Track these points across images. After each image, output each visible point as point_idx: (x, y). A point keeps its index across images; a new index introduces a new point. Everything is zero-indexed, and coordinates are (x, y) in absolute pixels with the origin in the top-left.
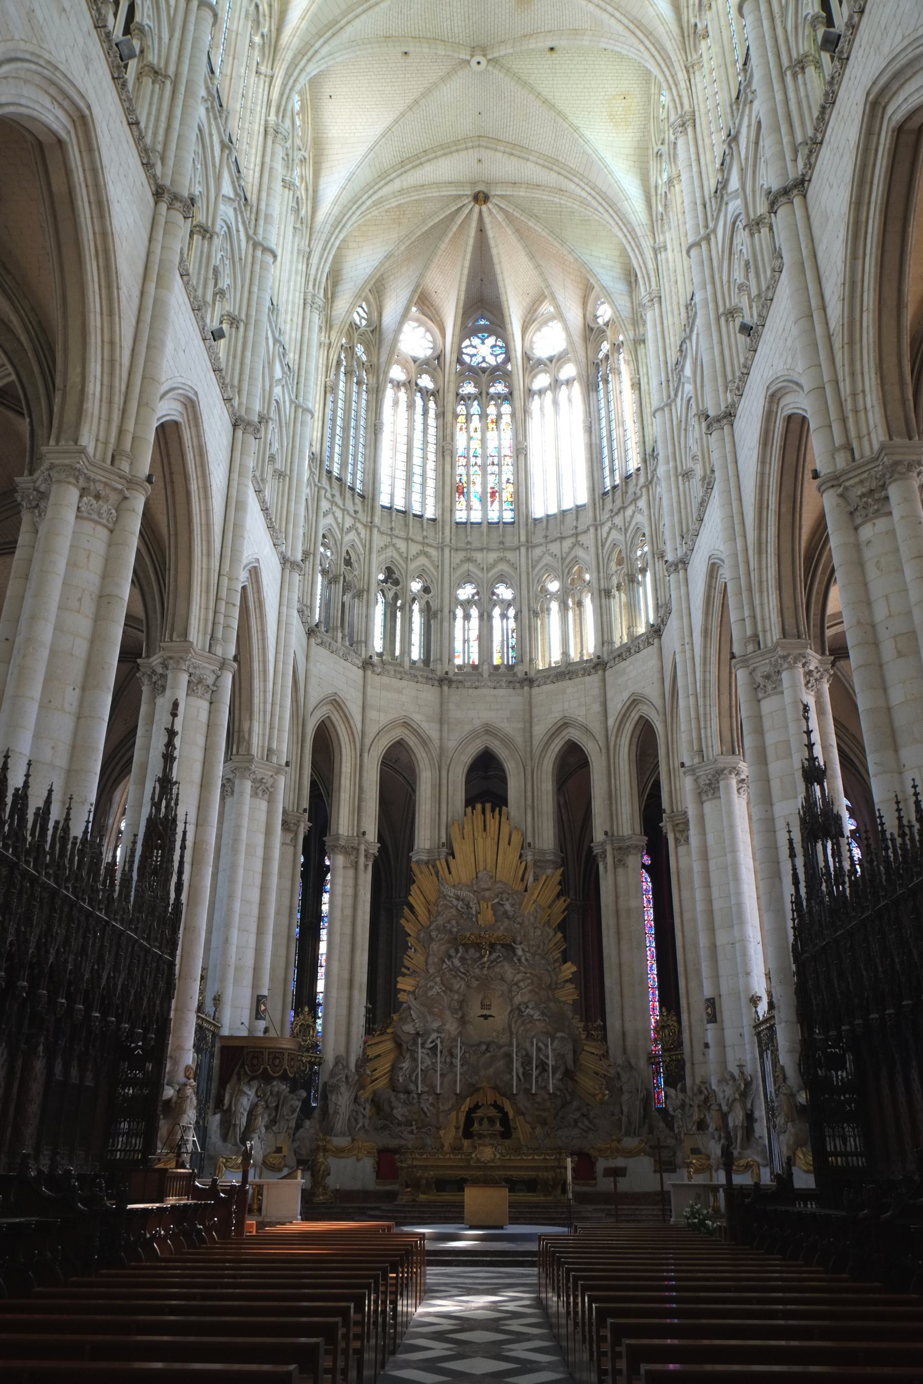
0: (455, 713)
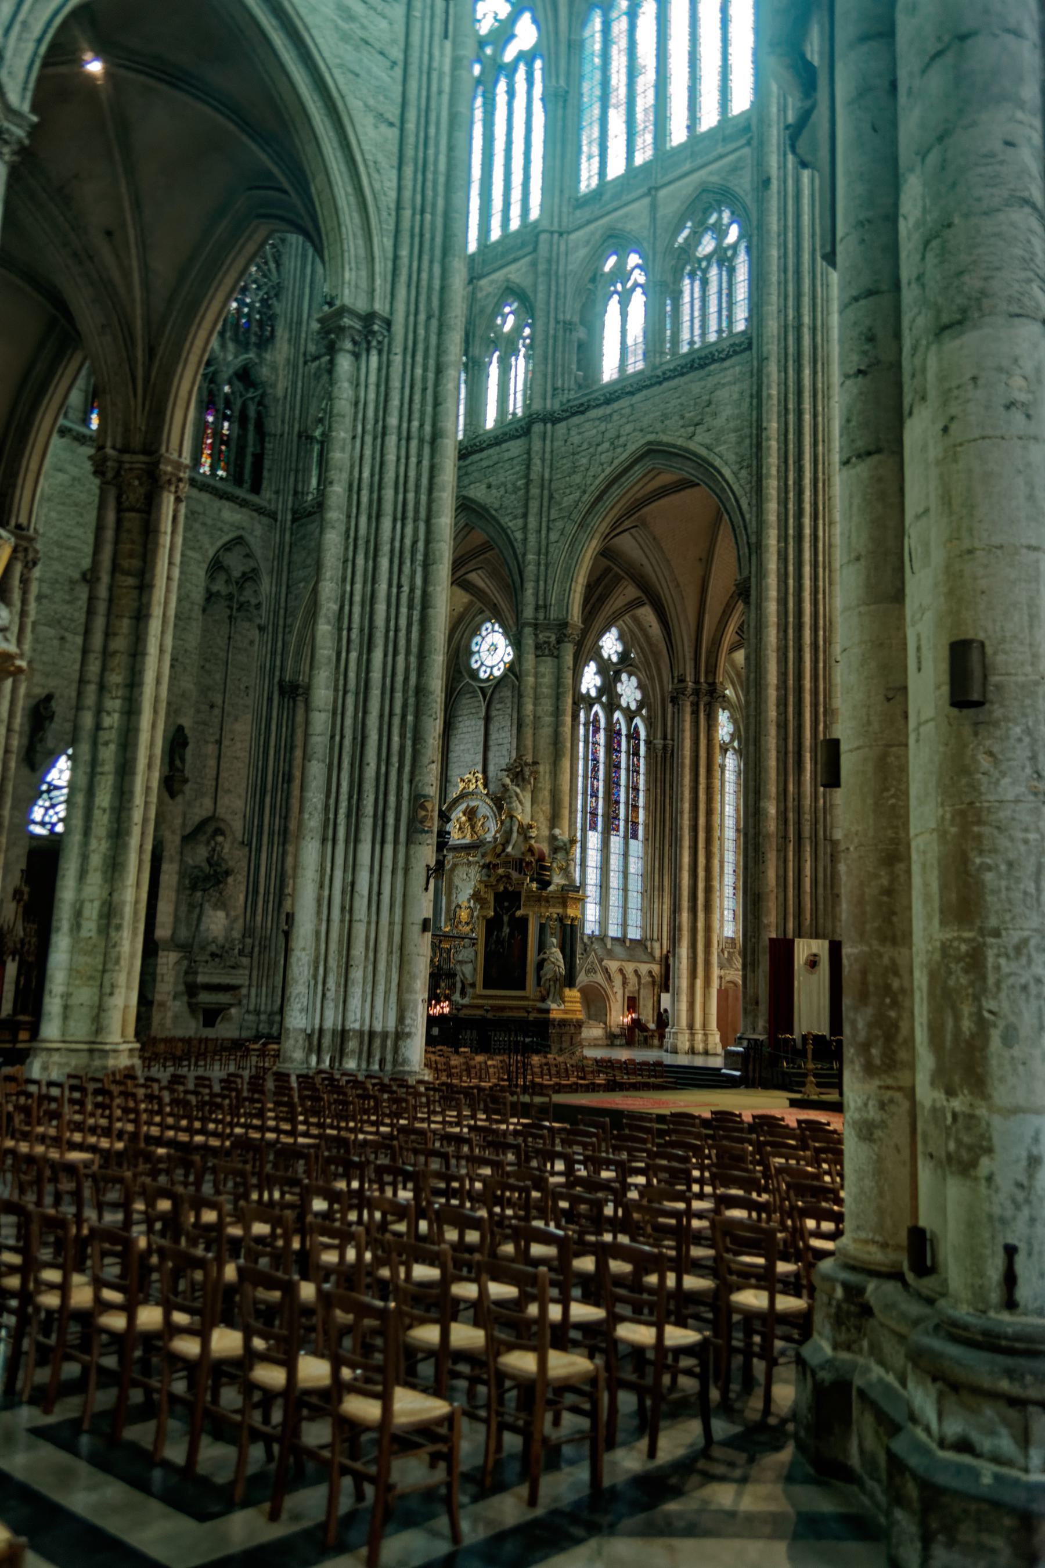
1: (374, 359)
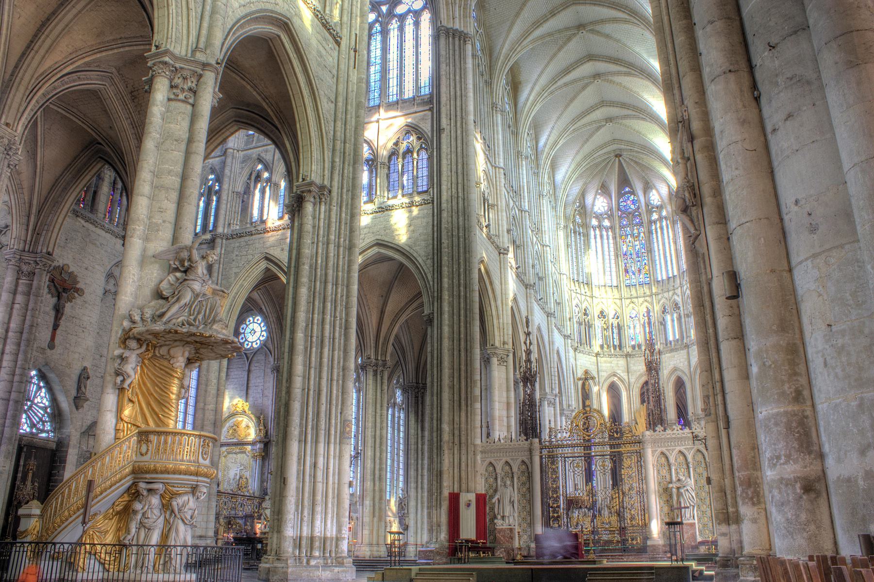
0: (633, 367)
1: (323, 207)
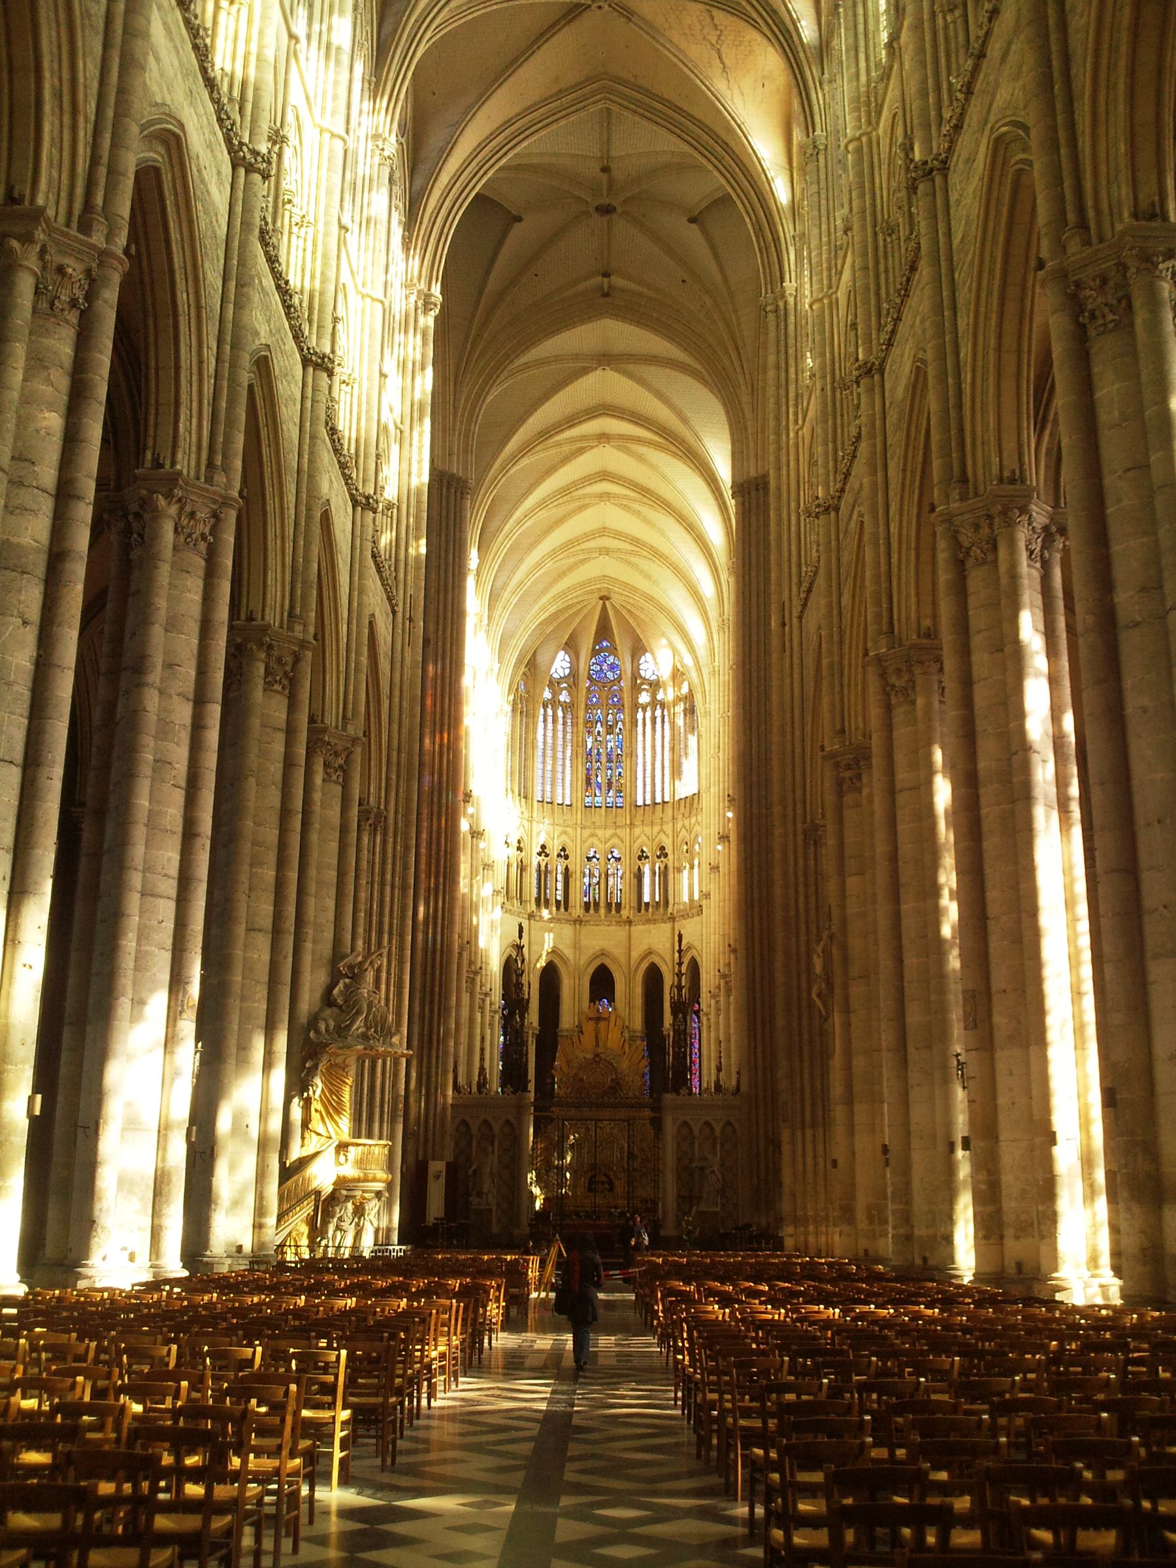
0: (584, 942)
